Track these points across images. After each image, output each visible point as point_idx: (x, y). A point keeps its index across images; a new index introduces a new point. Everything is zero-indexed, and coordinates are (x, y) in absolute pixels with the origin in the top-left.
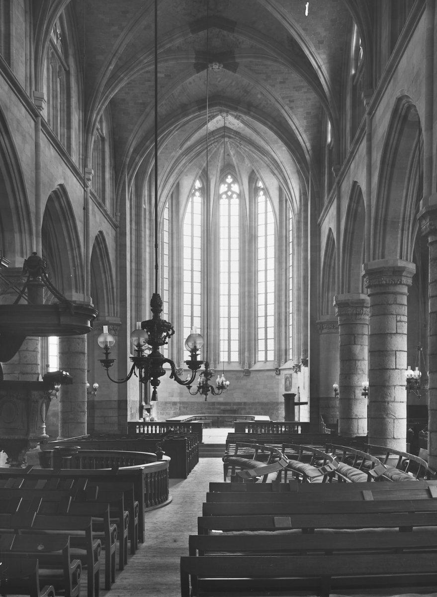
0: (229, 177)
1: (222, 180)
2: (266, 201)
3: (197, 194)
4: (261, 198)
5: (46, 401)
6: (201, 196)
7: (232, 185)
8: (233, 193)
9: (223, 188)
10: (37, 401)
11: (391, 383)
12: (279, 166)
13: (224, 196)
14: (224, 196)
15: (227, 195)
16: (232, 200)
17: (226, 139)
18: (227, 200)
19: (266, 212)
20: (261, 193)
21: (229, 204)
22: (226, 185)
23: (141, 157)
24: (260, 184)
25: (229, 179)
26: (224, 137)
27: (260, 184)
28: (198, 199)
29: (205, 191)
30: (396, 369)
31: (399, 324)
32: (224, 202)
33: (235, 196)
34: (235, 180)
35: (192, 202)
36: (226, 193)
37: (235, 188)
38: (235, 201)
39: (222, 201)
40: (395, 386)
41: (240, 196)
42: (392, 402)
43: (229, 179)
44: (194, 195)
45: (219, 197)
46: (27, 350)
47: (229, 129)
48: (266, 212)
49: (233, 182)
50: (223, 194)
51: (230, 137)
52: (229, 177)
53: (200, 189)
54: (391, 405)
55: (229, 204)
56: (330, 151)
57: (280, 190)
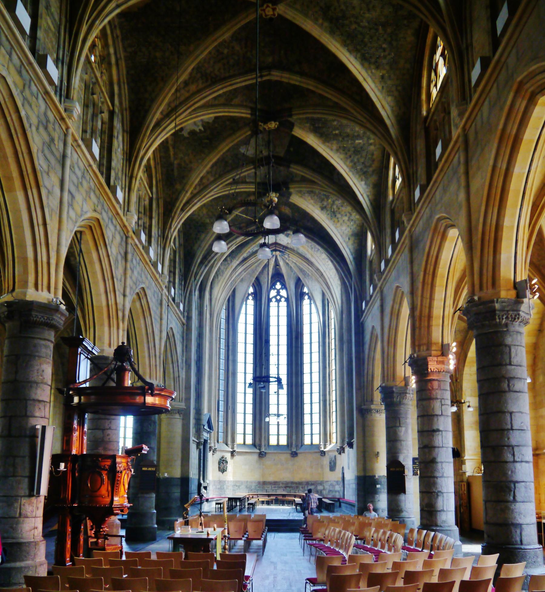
0: (278, 283)
1: (273, 286)
2: (311, 304)
3: (250, 297)
4: (306, 301)
5: (128, 472)
6: (253, 299)
7: (281, 291)
8: (281, 297)
9: (273, 293)
10: (121, 472)
11: (439, 460)
12: (322, 274)
13: (274, 300)
14: (274, 300)
16: (280, 303)
17: (278, 253)
18: (276, 303)
19: (311, 313)
20: (306, 297)
21: (278, 306)
22: (276, 291)
23: (206, 266)
24: (306, 290)
25: (278, 286)
26: (275, 250)
27: (306, 290)
28: (251, 302)
29: (257, 296)
30: (443, 447)
31: (443, 407)
32: (273, 304)
33: (283, 299)
34: (284, 286)
35: (246, 304)
36: (275, 297)
37: (283, 293)
38: (283, 304)
39: (272, 304)
40: (442, 462)
41: (287, 300)
42: (441, 477)
43: (278, 286)
44: (248, 298)
45: (269, 300)
46: (110, 428)
47: (280, 245)
48: (311, 313)
49: (282, 288)
50: (272, 298)
51: (280, 251)
52: (278, 283)
53: (252, 293)
54: (439, 480)
55: (278, 306)
56: (371, 262)
57: (323, 295)
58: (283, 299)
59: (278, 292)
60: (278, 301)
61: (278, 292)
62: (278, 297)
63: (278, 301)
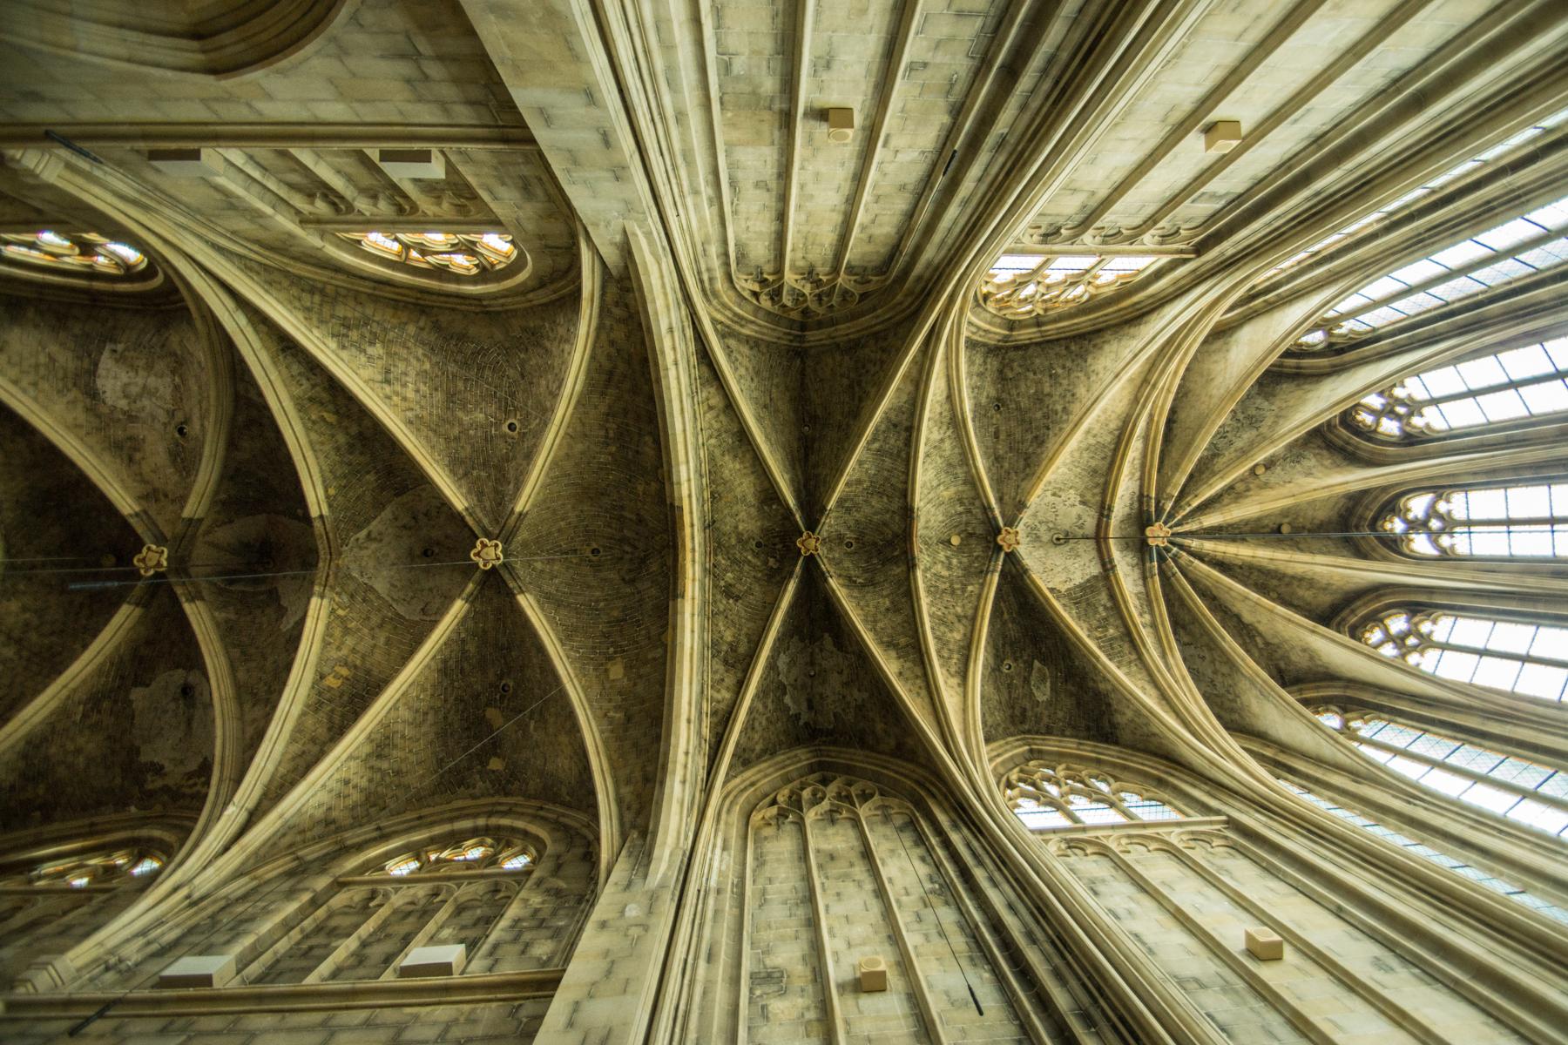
0: (1388, 526)
1: (1394, 545)
7: (1410, 516)
8: (1432, 512)
9: (1420, 544)
13: (1445, 541)
14: (1445, 541)
15: (1442, 531)
25: (1397, 526)
33: (1442, 507)
34: (1391, 505)
36: (1434, 536)
37: (1418, 506)
38: (1457, 505)
41: (1440, 488)
43: (1397, 526)
45: (1446, 557)
49: (1400, 512)
52: (1388, 526)
58: (1442, 507)
59: (1419, 525)
60: (1449, 525)
61: (1419, 525)
62: (1435, 524)
63: (1449, 525)
